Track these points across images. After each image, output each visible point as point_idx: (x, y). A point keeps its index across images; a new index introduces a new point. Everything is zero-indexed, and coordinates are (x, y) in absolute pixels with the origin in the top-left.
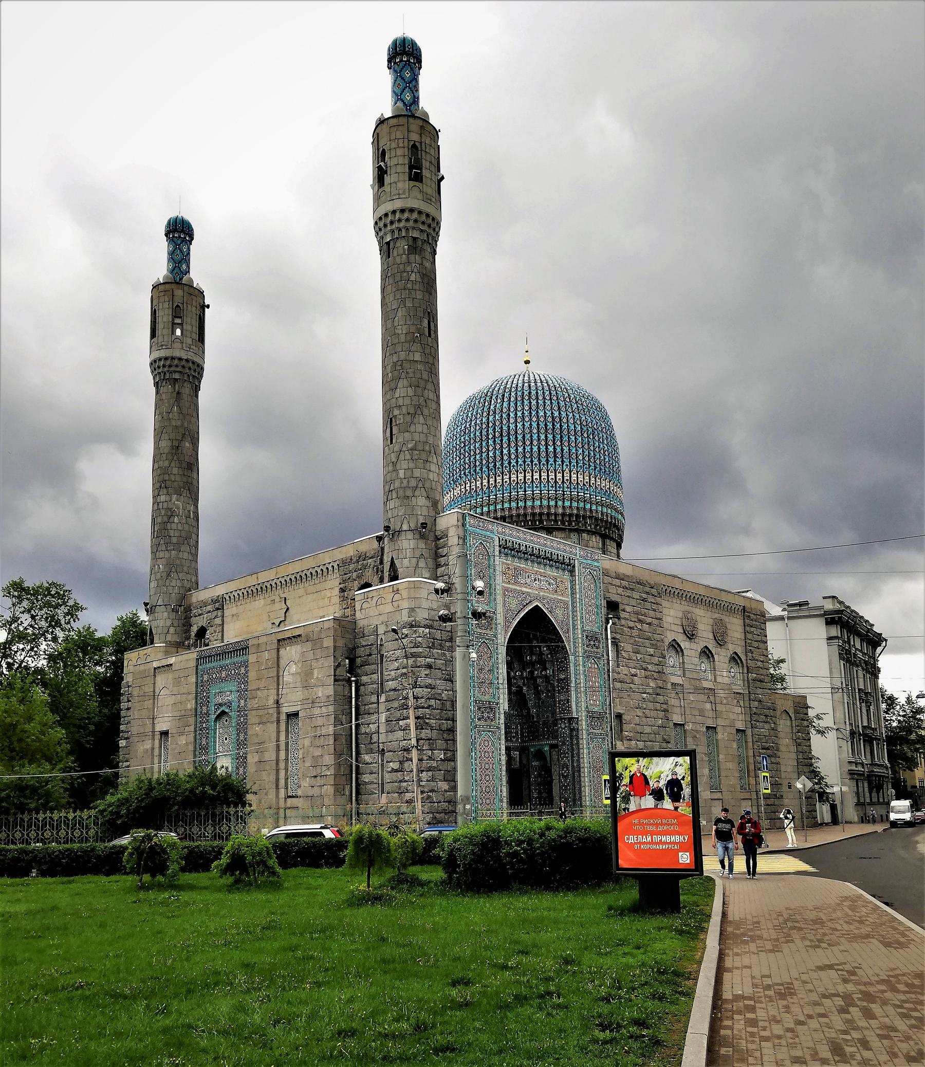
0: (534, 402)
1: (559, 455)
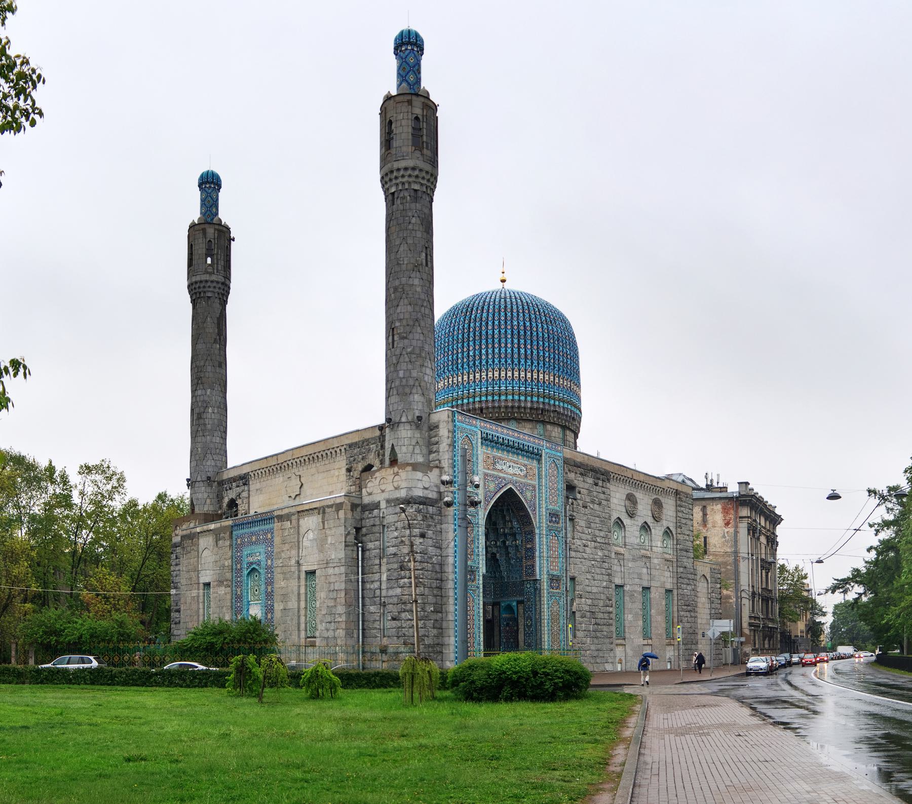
0: (509, 314)
1: (529, 357)
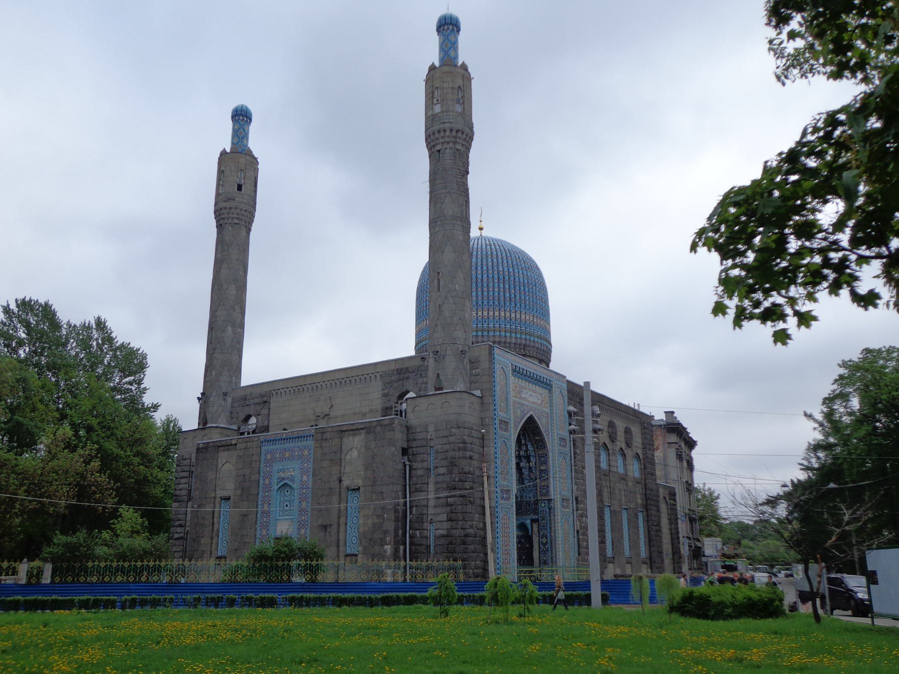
0: (495, 260)
